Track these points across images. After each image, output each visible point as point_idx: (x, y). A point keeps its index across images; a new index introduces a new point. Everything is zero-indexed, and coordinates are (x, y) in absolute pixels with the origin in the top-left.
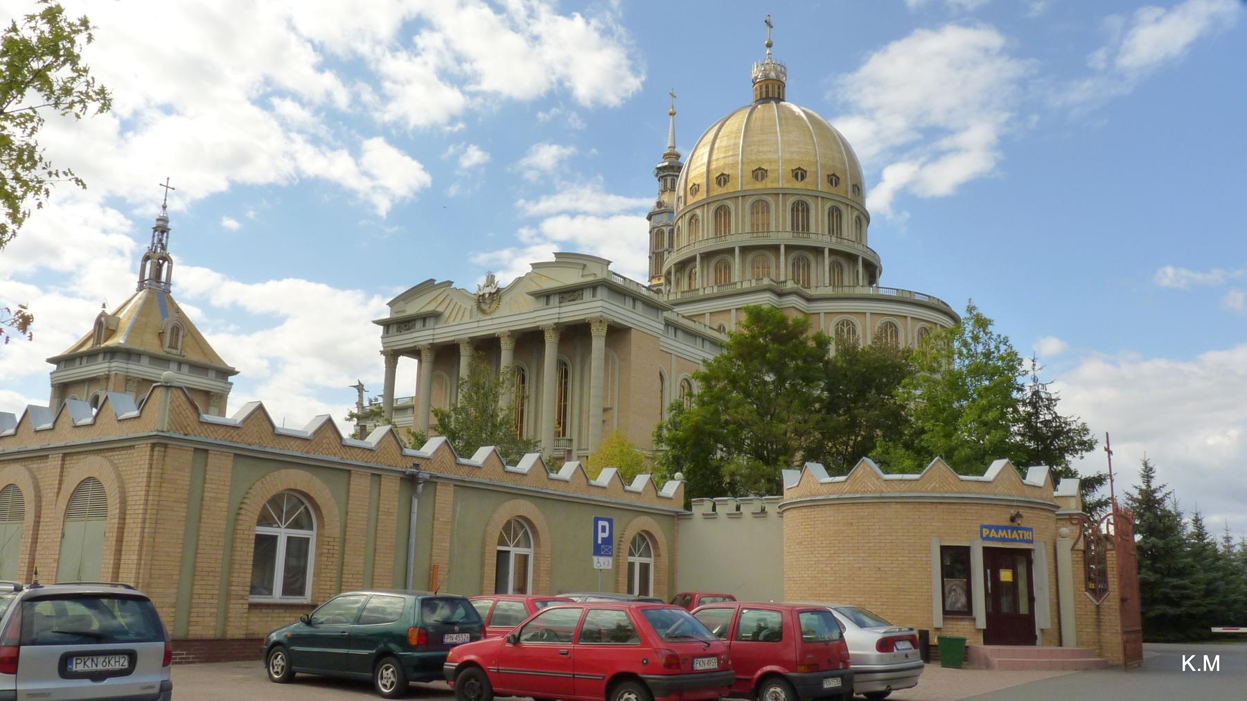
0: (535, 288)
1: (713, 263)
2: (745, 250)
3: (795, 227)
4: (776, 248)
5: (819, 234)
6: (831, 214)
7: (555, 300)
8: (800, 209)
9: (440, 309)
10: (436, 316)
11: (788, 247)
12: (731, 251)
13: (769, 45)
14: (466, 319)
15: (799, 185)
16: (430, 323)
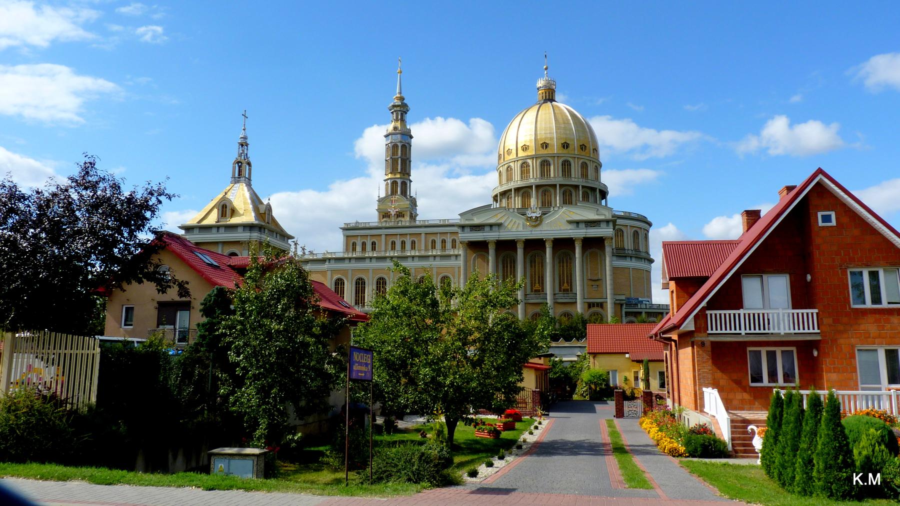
0: (569, 219)
1: (521, 193)
2: (538, 187)
3: (564, 175)
4: (554, 186)
5: (576, 178)
6: (582, 167)
7: (582, 225)
8: (566, 165)
9: (500, 221)
10: (499, 225)
11: (560, 185)
12: (531, 187)
13: (546, 69)
14: (521, 228)
15: (565, 151)
16: (494, 228)
